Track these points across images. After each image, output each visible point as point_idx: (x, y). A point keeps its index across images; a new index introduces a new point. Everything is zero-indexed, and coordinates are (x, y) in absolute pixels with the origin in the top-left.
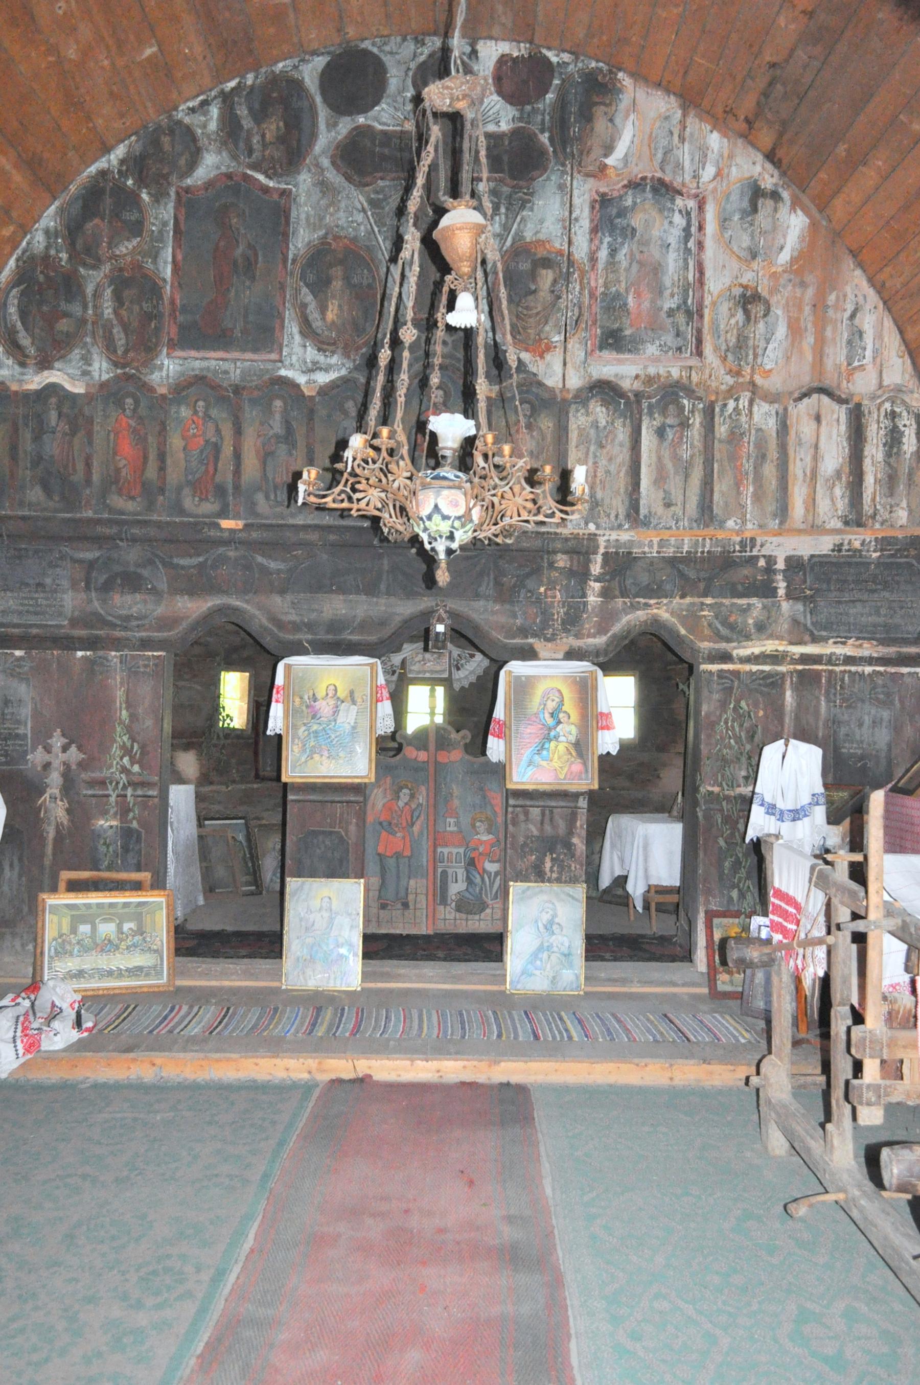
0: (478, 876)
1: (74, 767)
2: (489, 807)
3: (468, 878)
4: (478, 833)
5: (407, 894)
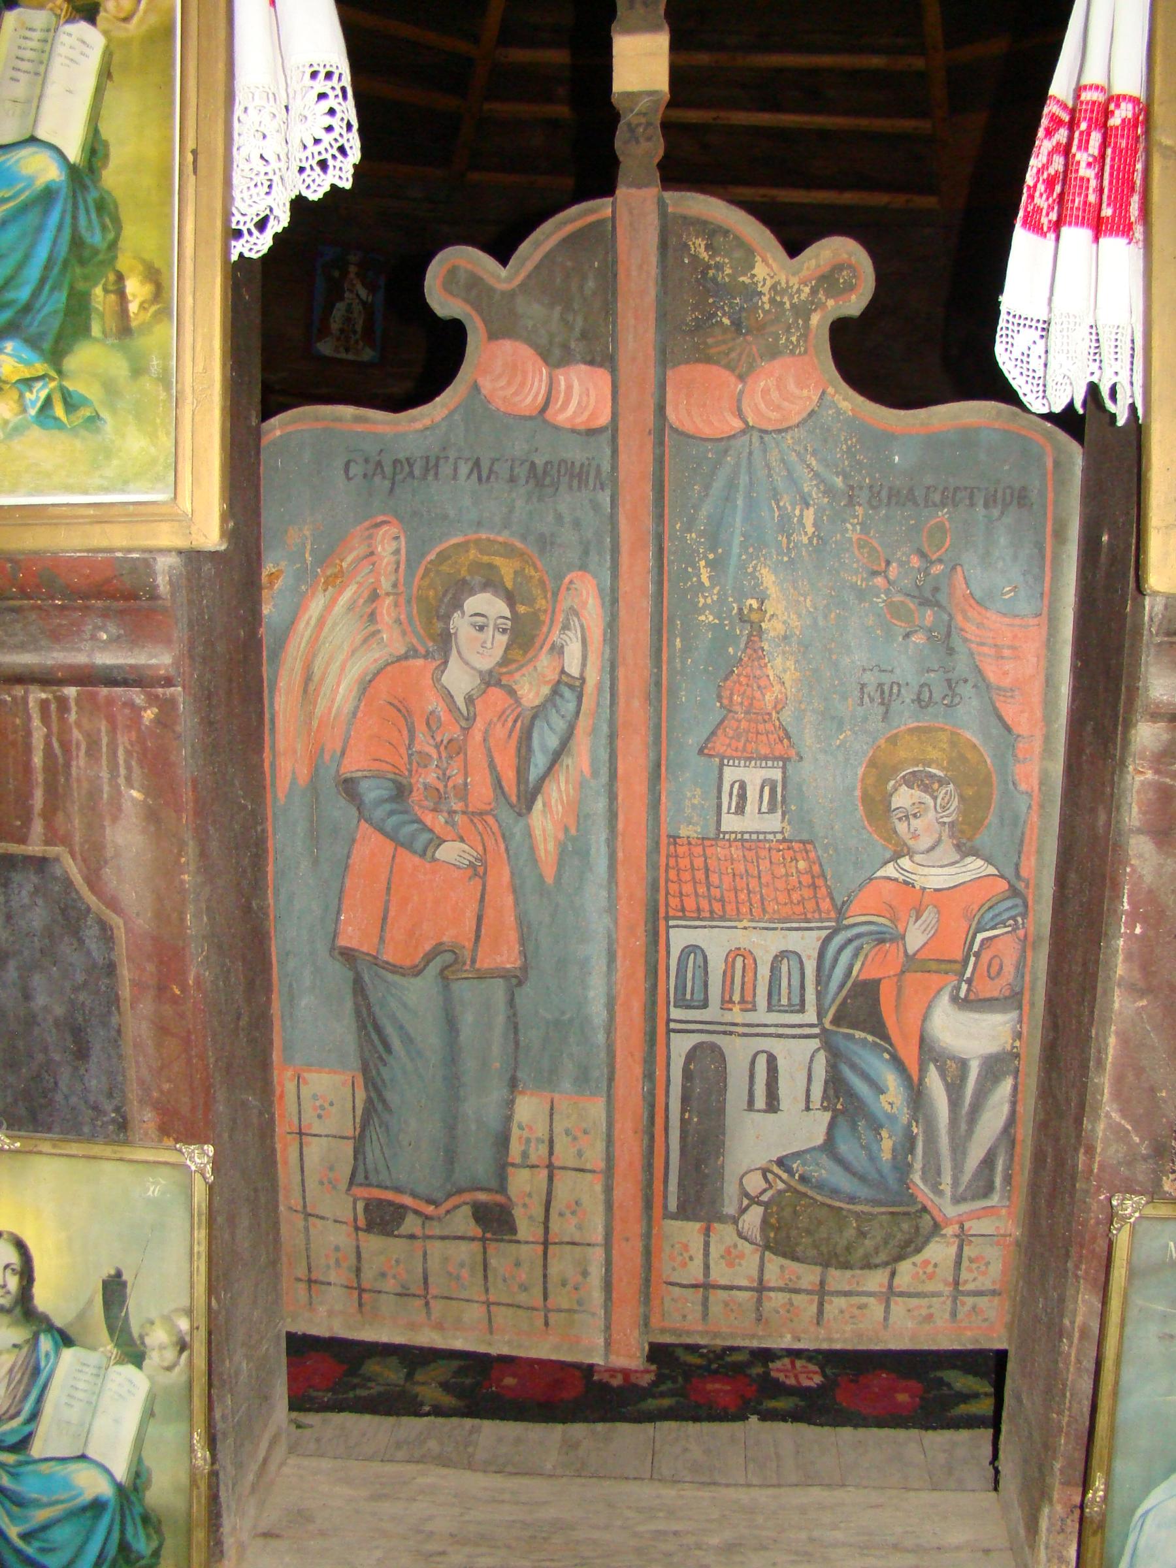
0: (891, 1080)
2: (970, 706)
3: (836, 1085)
5: (502, 1168)
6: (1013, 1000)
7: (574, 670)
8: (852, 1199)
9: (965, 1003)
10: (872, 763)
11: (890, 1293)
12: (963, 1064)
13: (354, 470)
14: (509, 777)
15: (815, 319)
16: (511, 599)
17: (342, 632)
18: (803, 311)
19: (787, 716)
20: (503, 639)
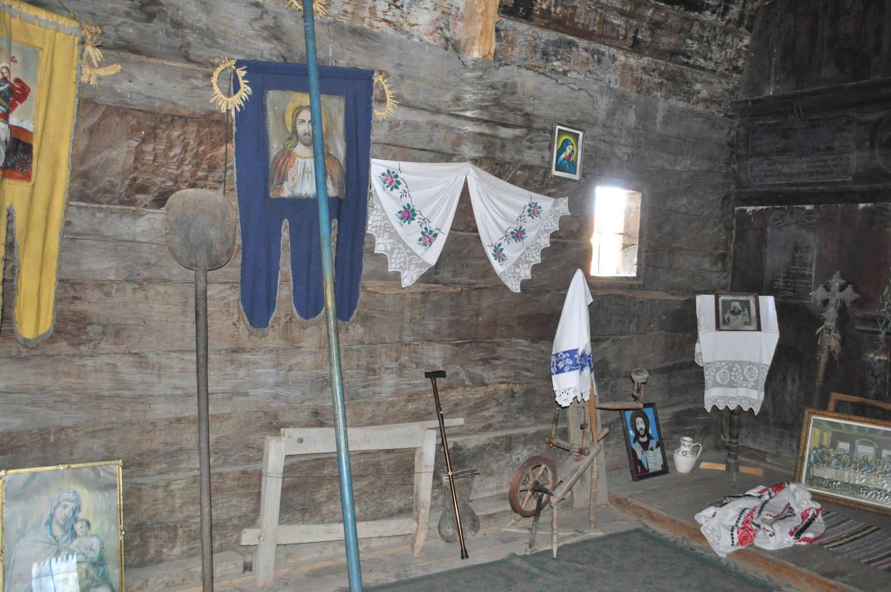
1: (848, 305)
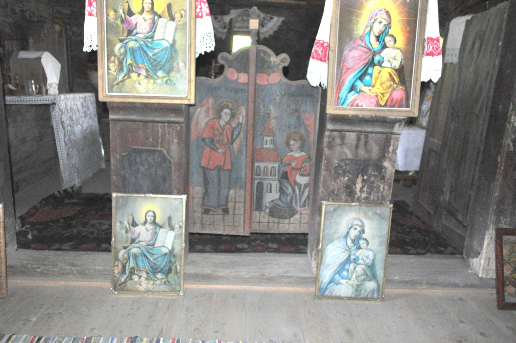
0: (290, 188)
2: (303, 127)
4: (291, 151)
6: (309, 175)
7: (241, 121)
8: (283, 207)
9: (302, 175)
10: (287, 137)
11: (289, 223)
12: (301, 185)
13: (206, 88)
14: (230, 139)
15: (280, 67)
16: (231, 110)
17: (203, 115)
18: (278, 65)
19: (274, 129)
20: (229, 116)
